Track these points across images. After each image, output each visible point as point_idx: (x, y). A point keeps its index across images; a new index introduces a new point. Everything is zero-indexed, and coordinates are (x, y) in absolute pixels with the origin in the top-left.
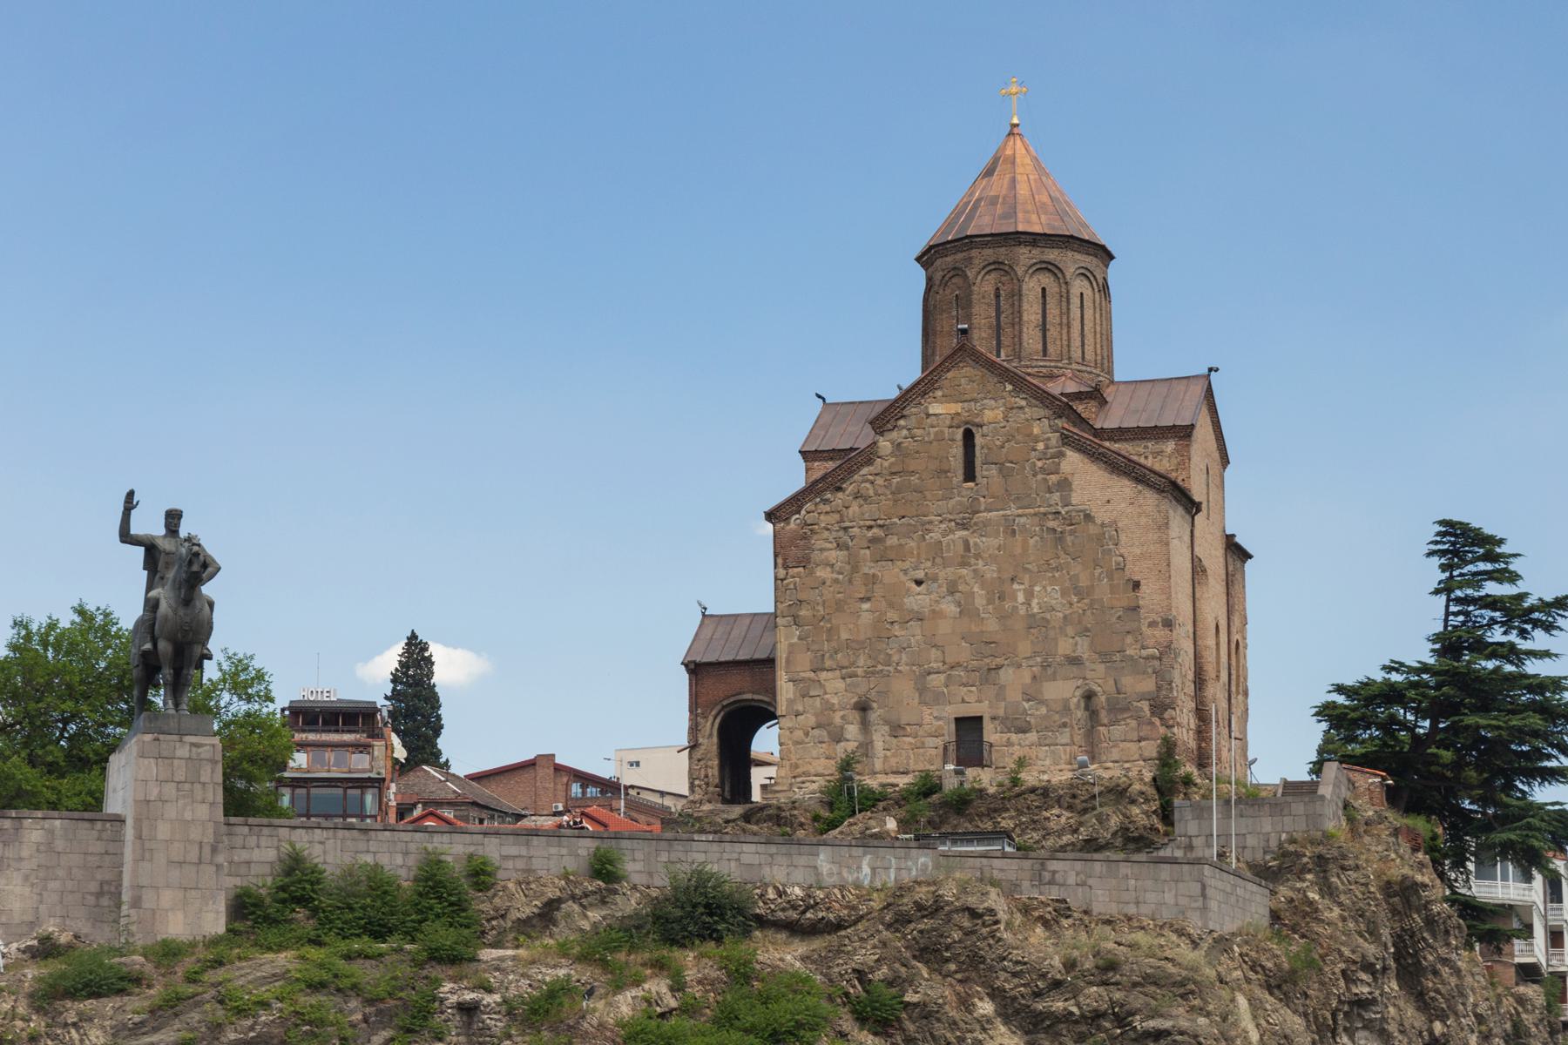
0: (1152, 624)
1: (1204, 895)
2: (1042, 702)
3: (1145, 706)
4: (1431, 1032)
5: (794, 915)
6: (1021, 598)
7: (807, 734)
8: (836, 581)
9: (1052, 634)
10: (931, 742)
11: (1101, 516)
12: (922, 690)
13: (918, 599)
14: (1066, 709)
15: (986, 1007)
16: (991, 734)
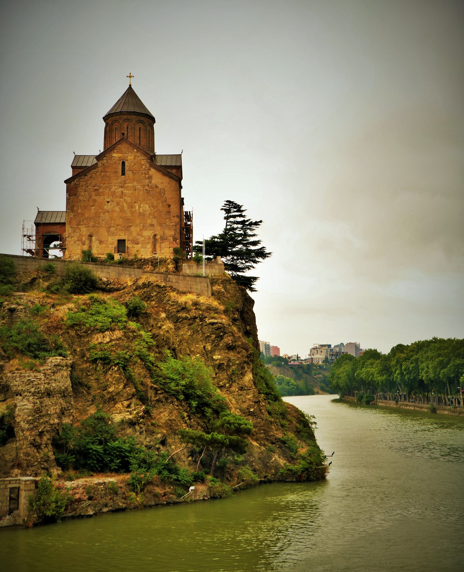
0: (174, 216)
1: (208, 287)
2: (142, 236)
3: (171, 239)
4: (246, 329)
5: (104, 286)
6: (137, 208)
7: (75, 243)
8: (84, 201)
9: (146, 218)
10: (110, 246)
11: (161, 186)
12: (108, 231)
13: (108, 207)
14: (149, 238)
15: (163, 315)
16: (128, 244)
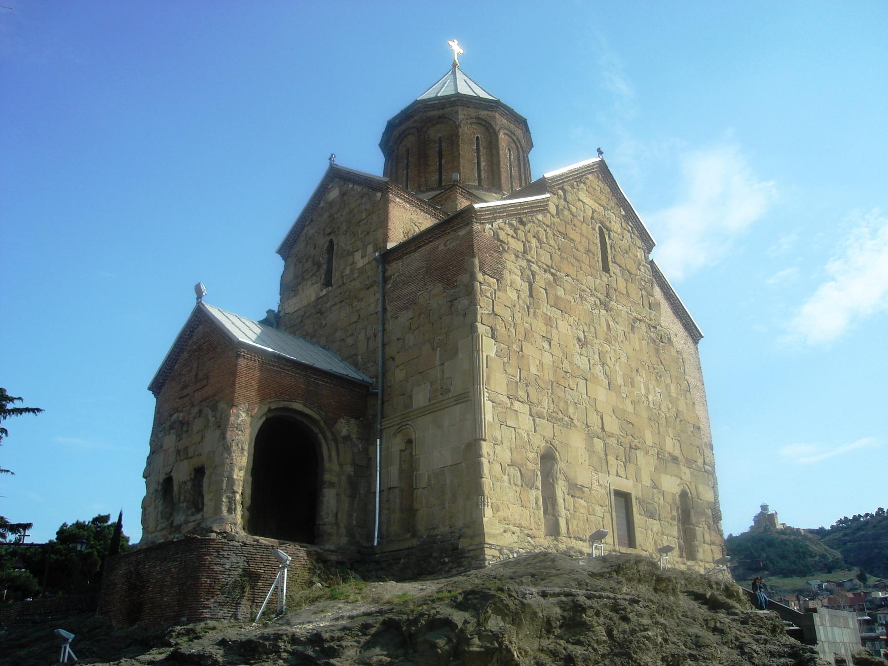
3: (709, 512)
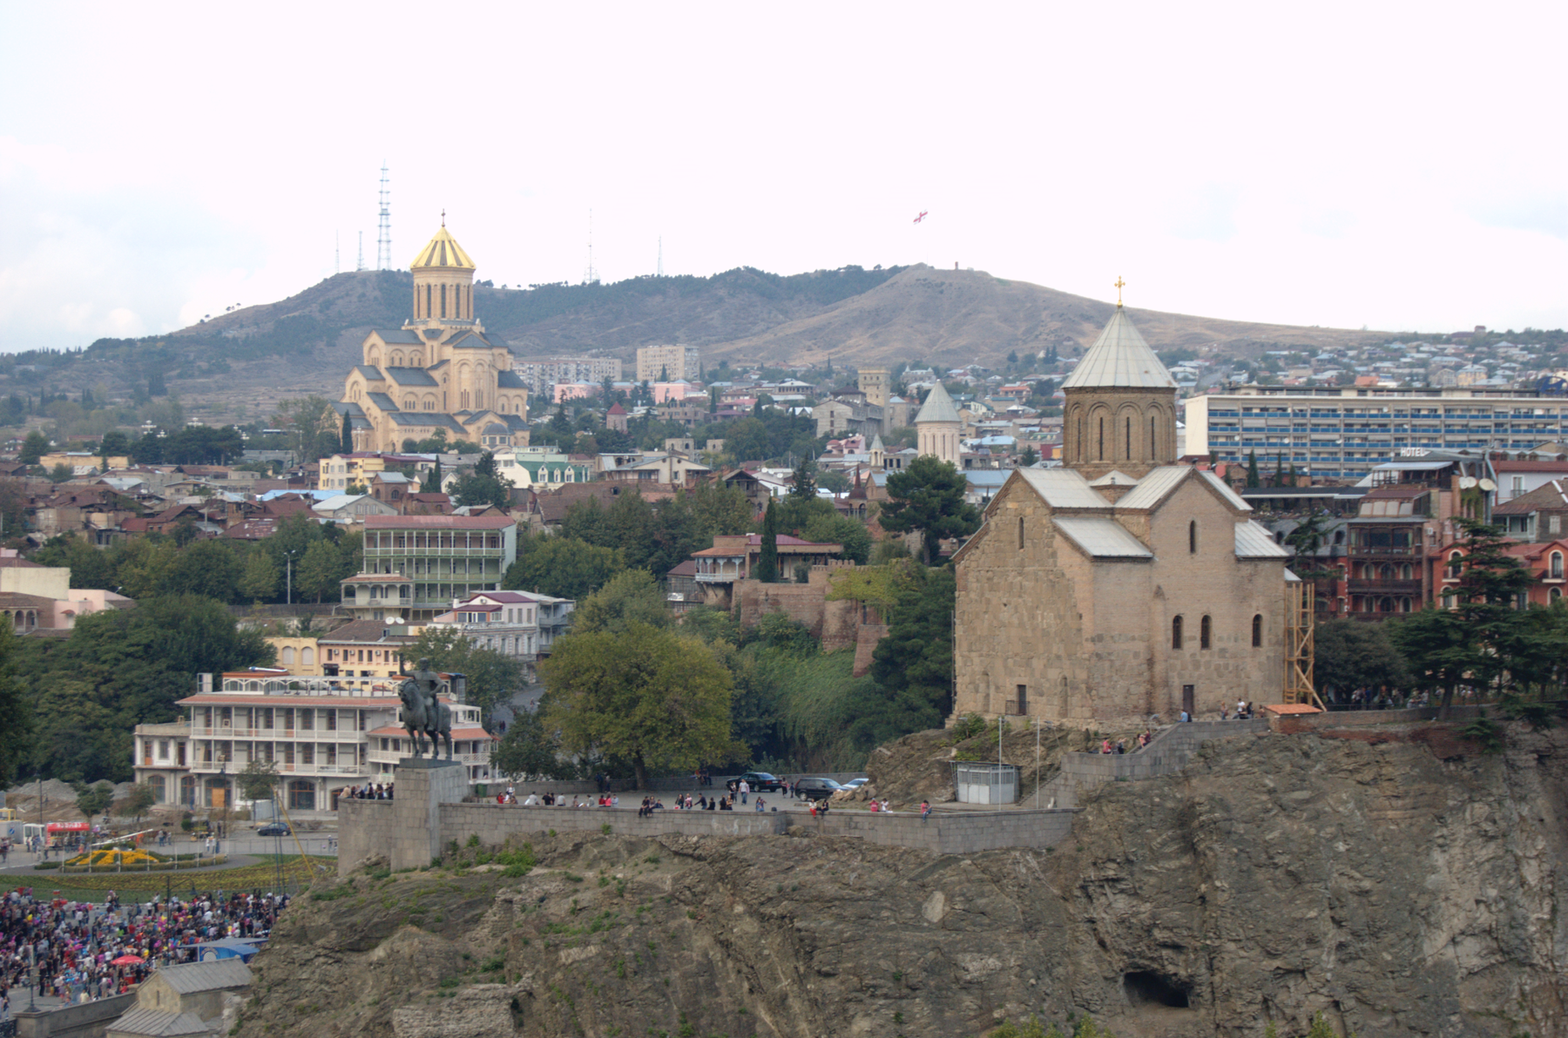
12: (1006, 667)
13: (1005, 615)
15: (739, 909)
16: (1030, 697)
